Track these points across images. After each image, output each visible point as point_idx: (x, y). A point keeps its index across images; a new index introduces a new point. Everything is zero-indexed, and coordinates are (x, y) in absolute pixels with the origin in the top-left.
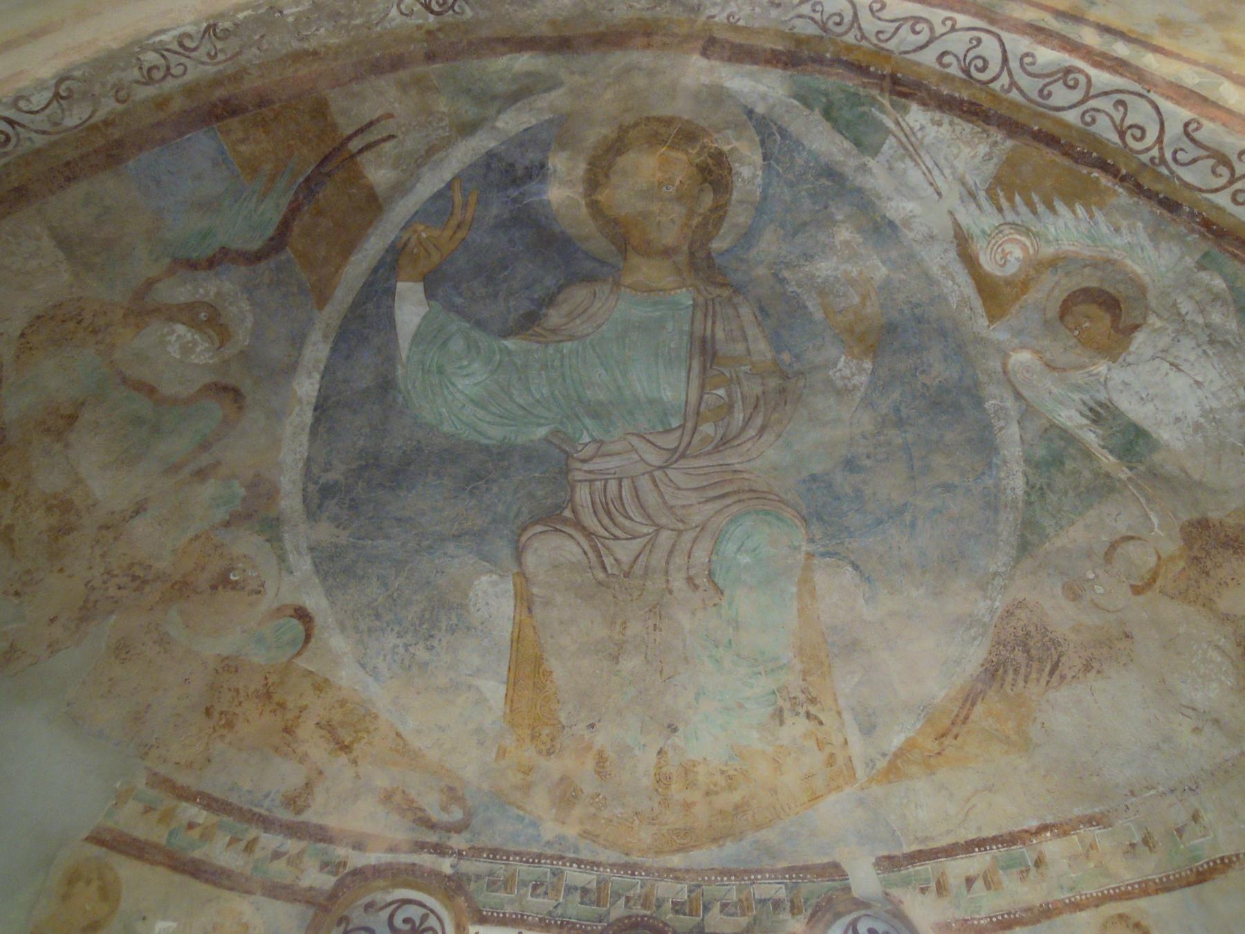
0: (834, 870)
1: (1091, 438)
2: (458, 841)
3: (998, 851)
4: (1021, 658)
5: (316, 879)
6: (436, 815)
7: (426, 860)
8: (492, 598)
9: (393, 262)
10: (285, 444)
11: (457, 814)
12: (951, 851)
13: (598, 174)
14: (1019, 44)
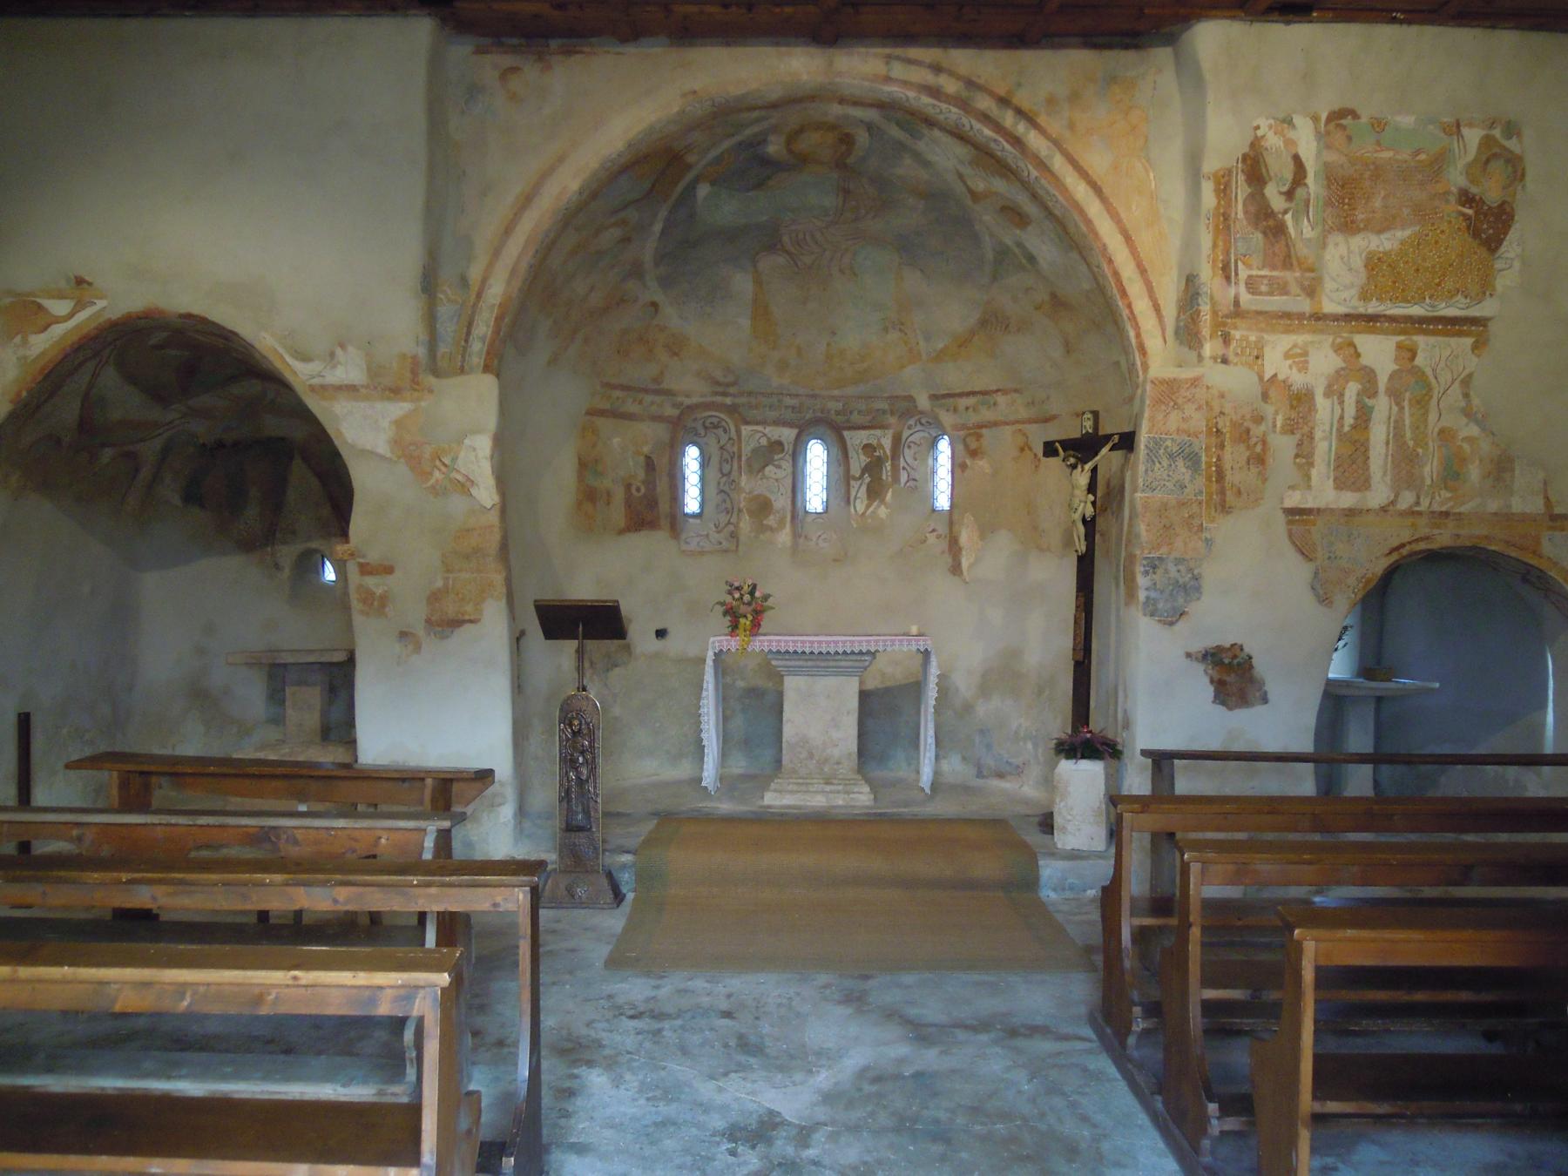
0: (910, 399)
1: (1016, 250)
2: (732, 390)
3: (980, 397)
4: (992, 322)
5: (670, 411)
6: (722, 379)
7: (719, 399)
8: (742, 283)
9: (697, 180)
10: (648, 249)
11: (730, 379)
12: (961, 395)
13: (792, 138)
14: (977, 125)
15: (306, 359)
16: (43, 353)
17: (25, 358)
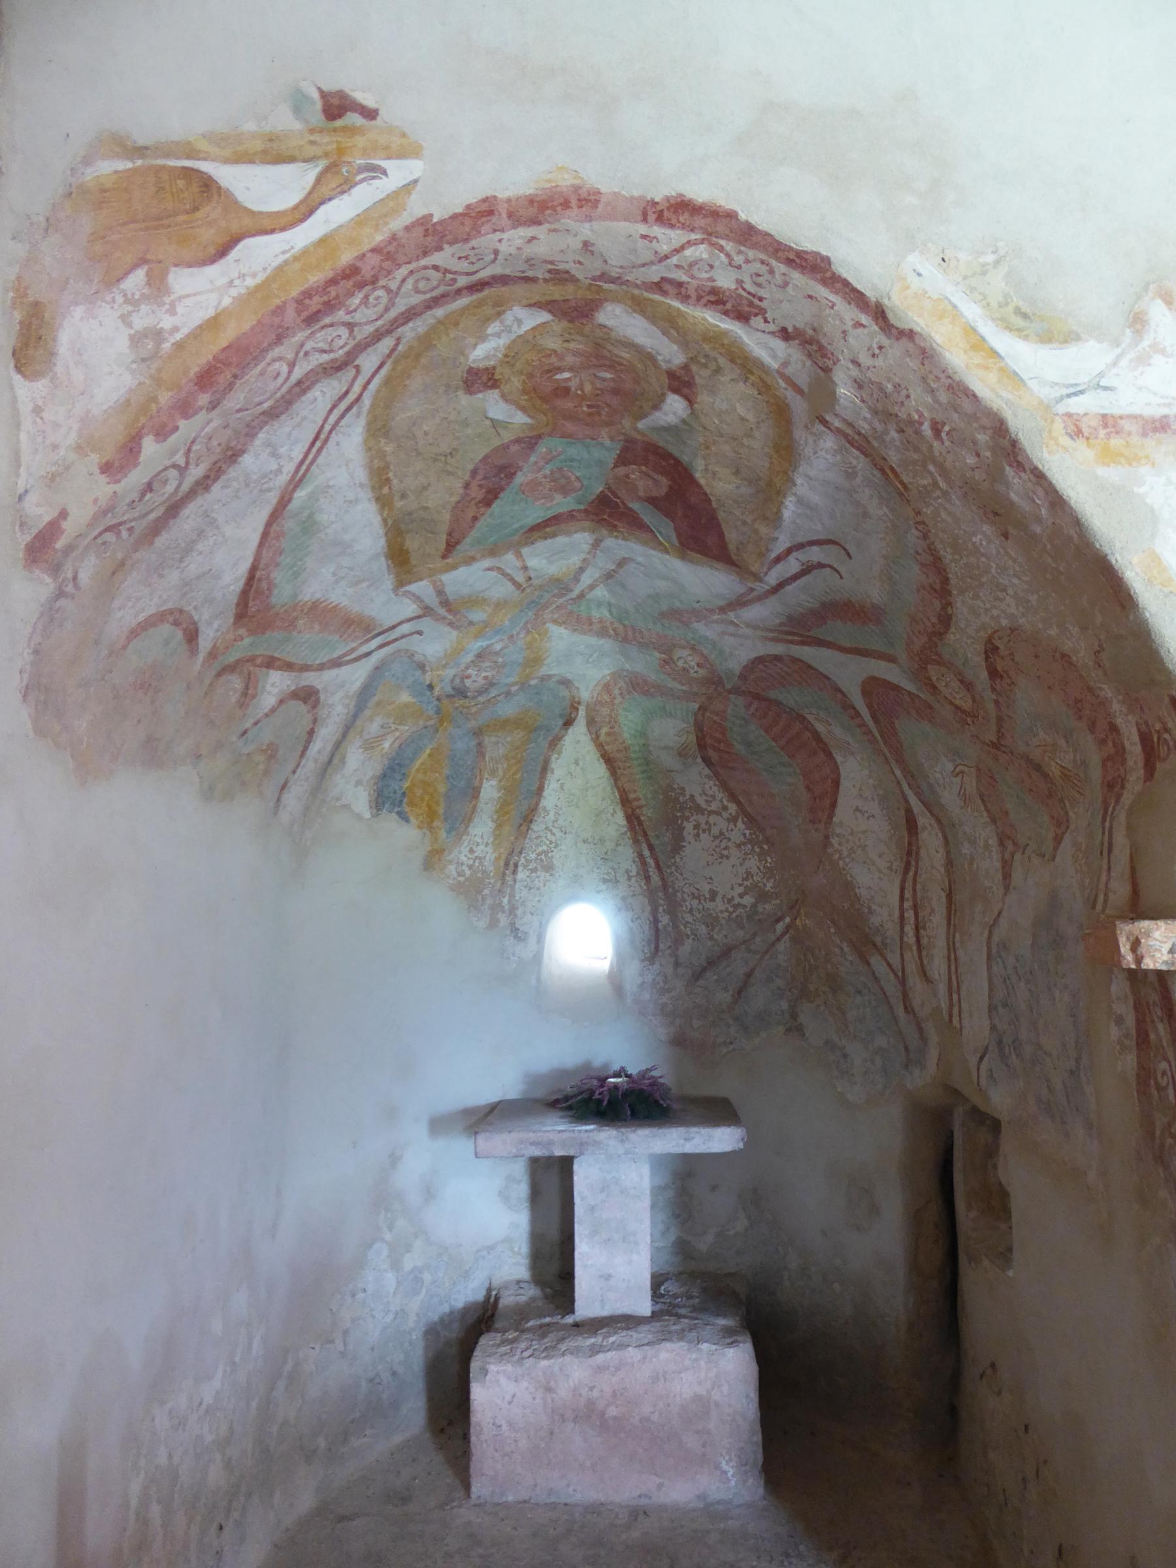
15: (1053, 332)
16: (214, 324)
17: (158, 335)
